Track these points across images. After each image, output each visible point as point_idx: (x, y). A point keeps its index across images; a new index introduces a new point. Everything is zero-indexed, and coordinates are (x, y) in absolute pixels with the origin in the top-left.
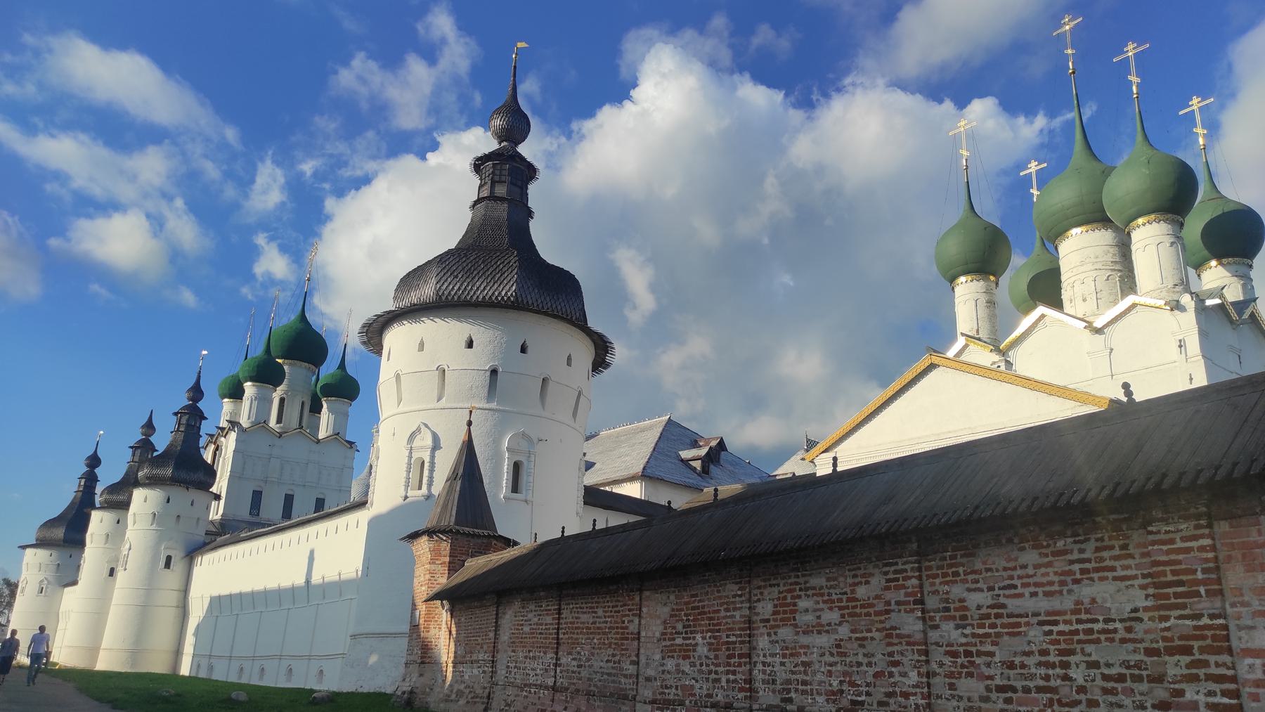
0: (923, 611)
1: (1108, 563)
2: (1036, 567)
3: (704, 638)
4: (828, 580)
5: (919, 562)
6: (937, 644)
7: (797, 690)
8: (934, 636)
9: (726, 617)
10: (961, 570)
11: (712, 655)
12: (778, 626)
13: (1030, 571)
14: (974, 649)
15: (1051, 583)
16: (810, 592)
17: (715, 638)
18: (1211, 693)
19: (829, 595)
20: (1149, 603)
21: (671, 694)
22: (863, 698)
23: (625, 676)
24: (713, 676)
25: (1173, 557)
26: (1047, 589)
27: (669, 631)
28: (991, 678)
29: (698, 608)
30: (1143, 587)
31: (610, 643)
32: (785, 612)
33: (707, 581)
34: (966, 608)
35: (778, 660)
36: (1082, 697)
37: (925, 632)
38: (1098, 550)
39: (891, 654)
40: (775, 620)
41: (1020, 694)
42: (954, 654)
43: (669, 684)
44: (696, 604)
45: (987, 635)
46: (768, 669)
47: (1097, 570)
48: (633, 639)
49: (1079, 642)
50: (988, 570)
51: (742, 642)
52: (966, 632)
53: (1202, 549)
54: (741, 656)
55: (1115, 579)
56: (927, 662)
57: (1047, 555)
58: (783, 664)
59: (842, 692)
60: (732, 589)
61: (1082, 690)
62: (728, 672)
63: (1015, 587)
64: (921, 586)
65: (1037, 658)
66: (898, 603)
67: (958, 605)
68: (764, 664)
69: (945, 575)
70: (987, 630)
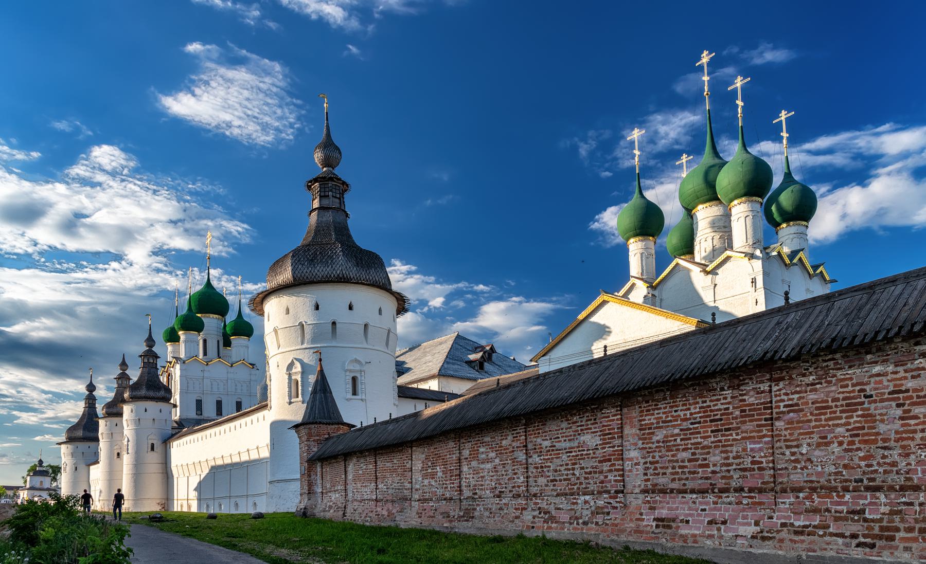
0: (526, 450)
1: (590, 426)
2: (566, 429)
3: (440, 469)
4: (491, 438)
5: (525, 428)
6: (531, 464)
7: (478, 489)
8: (530, 460)
9: (449, 458)
10: (541, 431)
11: (444, 476)
12: (471, 461)
13: (564, 431)
14: (544, 465)
15: (571, 436)
16: (484, 444)
17: (445, 468)
18: (615, 476)
19: (492, 445)
20: (601, 442)
21: (427, 496)
22: (504, 490)
23: (406, 489)
24: (445, 486)
25: (609, 423)
26: (569, 438)
27: (425, 466)
28: (549, 477)
29: (437, 454)
30: (600, 436)
31: (399, 474)
32: (474, 454)
33: (441, 441)
34: (542, 448)
35: (471, 476)
36: (578, 481)
37: (527, 459)
38: (587, 421)
39: (514, 470)
40: (470, 458)
41: (558, 482)
42: (537, 468)
43: (425, 491)
44: (437, 453)
45: (549, 459)
46: (467, 481)
47: (586, 429)
48: (409, 471)
49: (579, 459)
50: (550, 431)
51: (456, 469)
52: (542, 458)
53: (617, 419)
54: (456, 476)
55: (592, 433)
56: (527, 472)
57: (570, 424)
58: (473, 478)
59: (496, 488)
60: (451, 444)
61: (578, 478)
62: (451, 483)
63: (559, 438)
64: (526, 439)
65: (565, 467)
66: (517, 447)
67: (539, 446)
68: (466, 478)
69: (535, 434)
70: (549, 457)
